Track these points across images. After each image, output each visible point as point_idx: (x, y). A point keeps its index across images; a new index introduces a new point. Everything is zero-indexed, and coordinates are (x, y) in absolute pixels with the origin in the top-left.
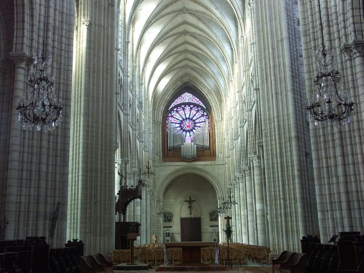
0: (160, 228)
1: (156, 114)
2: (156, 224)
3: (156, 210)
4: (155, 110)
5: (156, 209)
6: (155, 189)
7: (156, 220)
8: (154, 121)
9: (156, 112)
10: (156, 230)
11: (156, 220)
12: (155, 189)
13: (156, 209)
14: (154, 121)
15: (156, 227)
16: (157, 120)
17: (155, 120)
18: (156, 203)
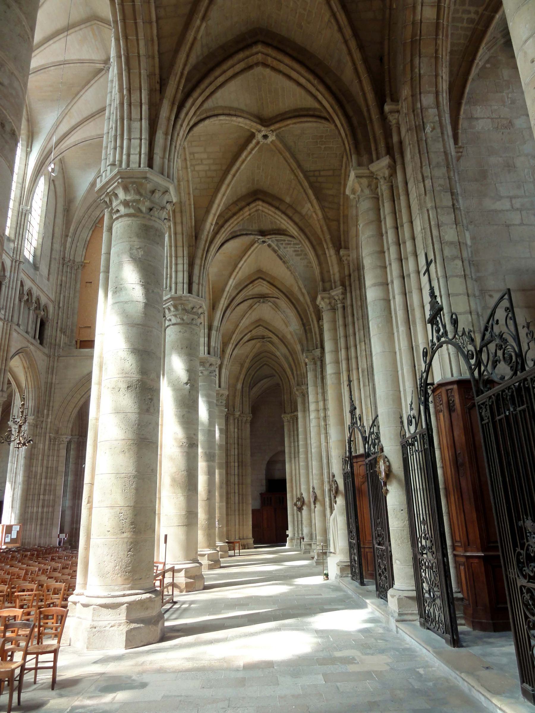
0: (53, 506)
1: (68, 245)
2: (41, 497)
3: (45, 462)
4: (67, 236)
5: (45, 458)
6: (48, 410)
7: (42, 487)
8: (64, 259)
9: (69, 240)
10: (40, 510)
11: (42, 487)
12: (48, 410)
13: (45, 458)
14: (64, 259)
15: (41, 504)
16: (72, 258)
17: (67, 255)
18: (47, 443)
